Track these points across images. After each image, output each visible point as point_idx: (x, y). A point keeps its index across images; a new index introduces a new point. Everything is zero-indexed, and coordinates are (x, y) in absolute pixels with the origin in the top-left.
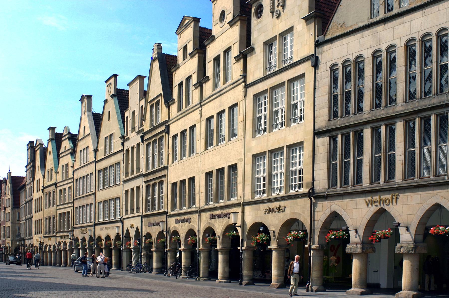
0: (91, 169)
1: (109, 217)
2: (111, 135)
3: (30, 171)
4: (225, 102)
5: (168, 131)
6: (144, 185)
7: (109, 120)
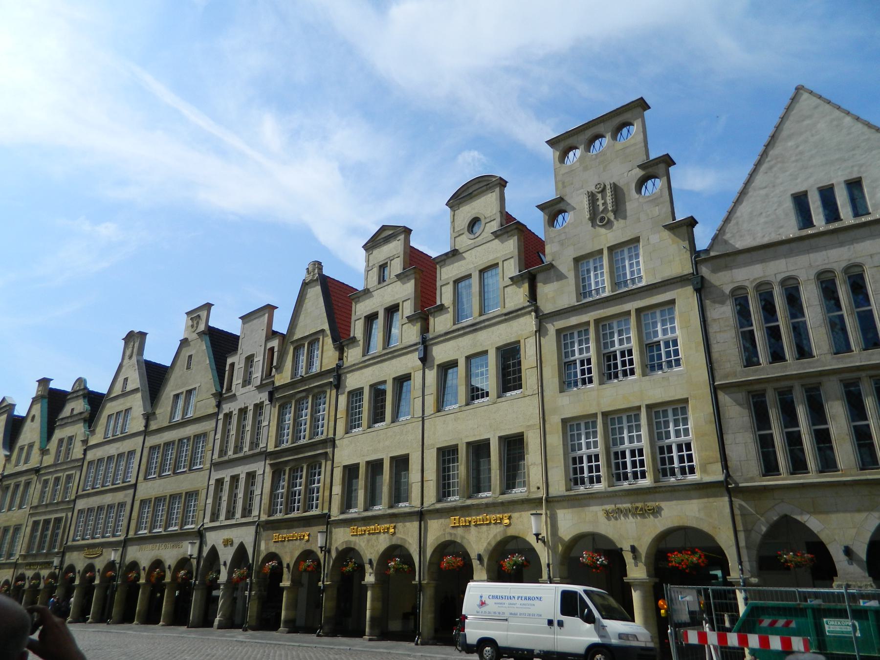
1: (168, 525)
2: (189, 392)
5: (338, 385)
7: (188, 368)
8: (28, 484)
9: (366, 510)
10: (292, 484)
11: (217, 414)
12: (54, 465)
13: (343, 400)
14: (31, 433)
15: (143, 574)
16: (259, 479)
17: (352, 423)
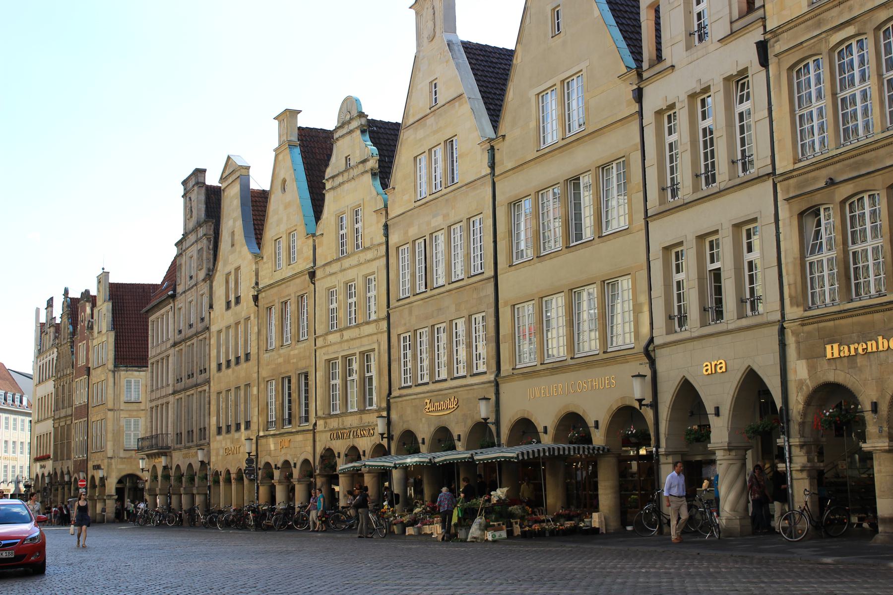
10: (850, 233)
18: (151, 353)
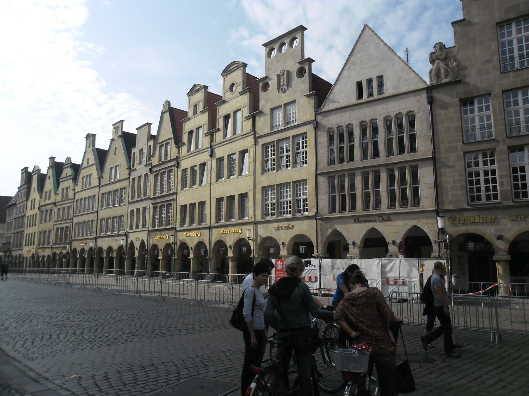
0: (95, 191)
2: (116, 166)
3: (23, 191)
4: (237, 147)
5: (178, 166)
6: (152, 206)
7: (115, 154)
8: (51, 210)
9: (190, 226)
11: (129, 178)
12: (62, 201)
13: (180, 174)
14: (49, 185)
15: (105, 253)
16: (147, 210)
17: (184, 186)
18: (7, 220)
